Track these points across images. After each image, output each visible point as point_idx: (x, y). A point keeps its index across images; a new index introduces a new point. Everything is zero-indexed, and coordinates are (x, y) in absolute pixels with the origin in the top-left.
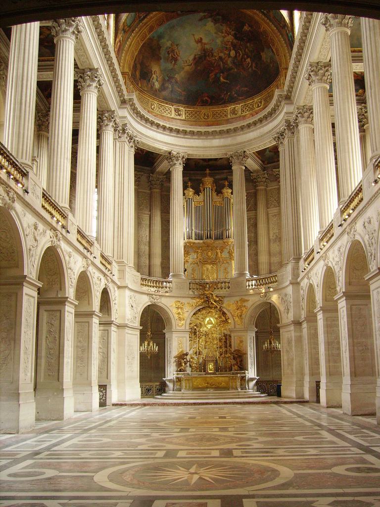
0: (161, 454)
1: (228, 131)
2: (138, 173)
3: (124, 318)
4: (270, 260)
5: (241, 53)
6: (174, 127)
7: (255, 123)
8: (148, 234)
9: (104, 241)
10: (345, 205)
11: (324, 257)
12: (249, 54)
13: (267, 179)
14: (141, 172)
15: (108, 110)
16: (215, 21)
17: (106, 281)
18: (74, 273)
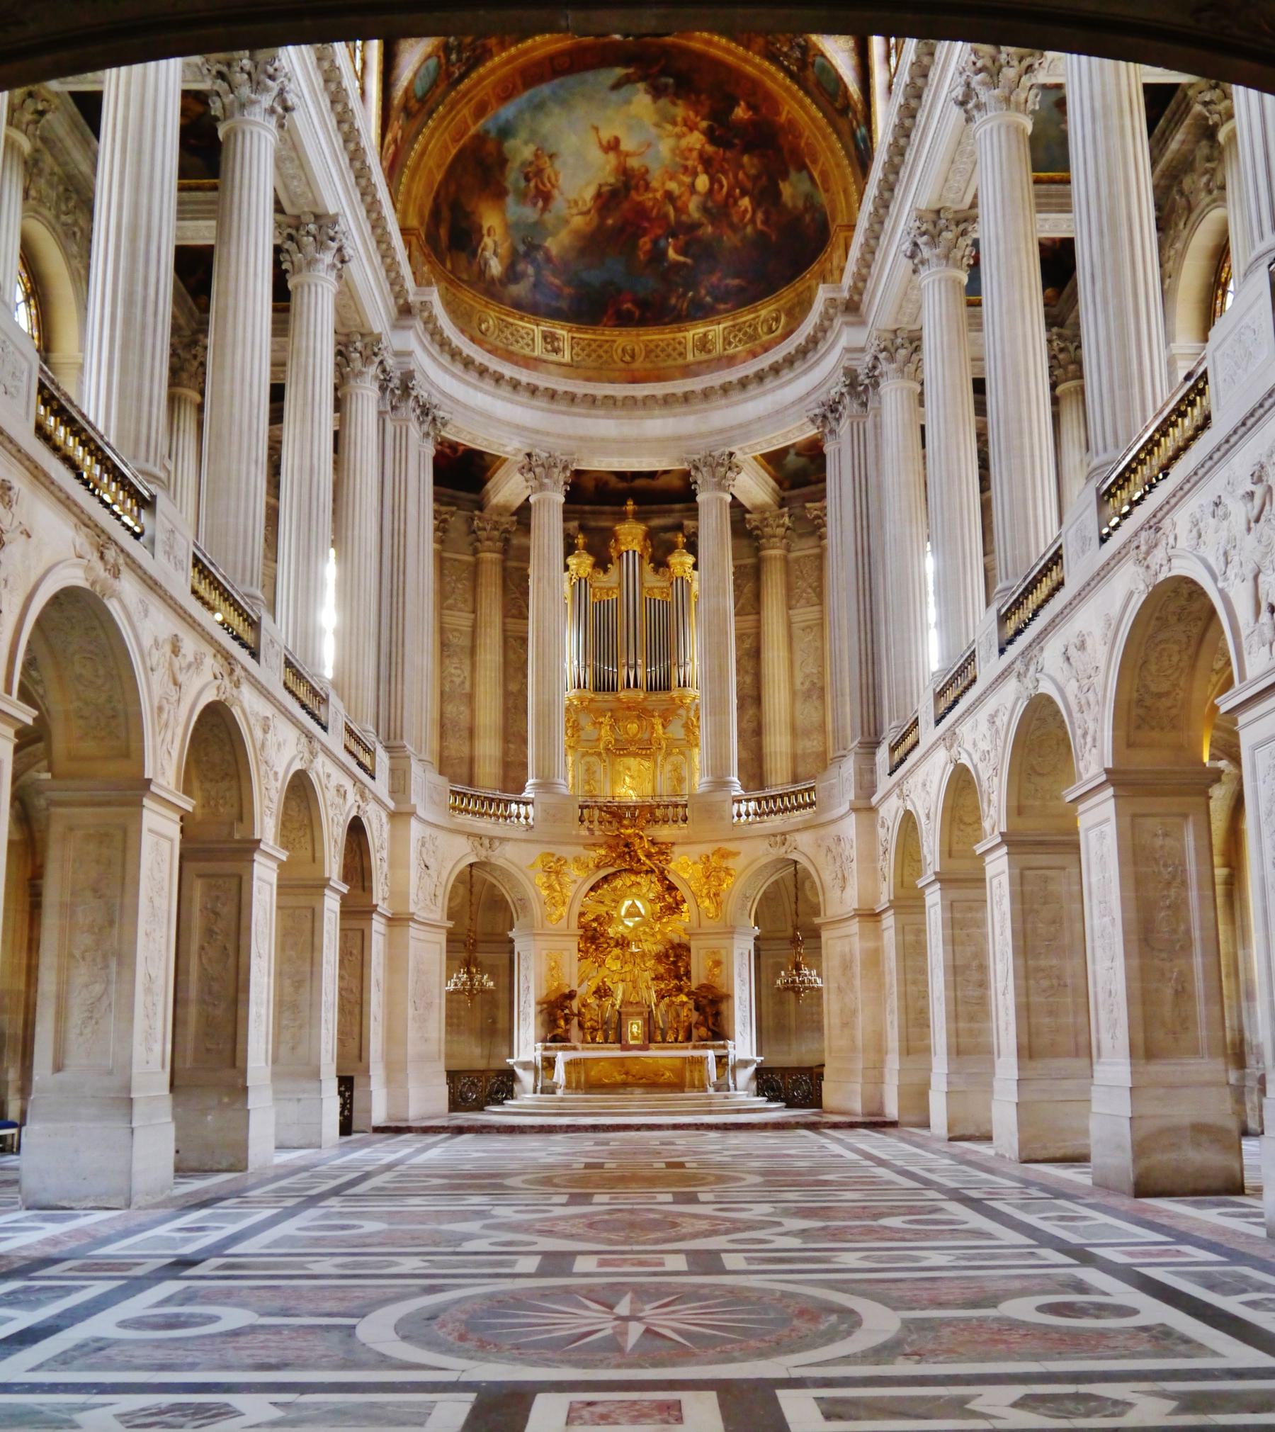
0: (529, 1264)
1: (687, 398)
2: (444, 509)
3: (405, 897)
4: (793, 746)
5: (725, 182)
7: (760, 377)
8: (467, 673)
9: (353, 691)
10: (1011, 601)
11: (950, 739)
12: (749, 185)
13: (788, 528)
14: (449, 504)
15: (363, 331)
16: (657, 92)
17: (358, 798)
18: (276, 773)
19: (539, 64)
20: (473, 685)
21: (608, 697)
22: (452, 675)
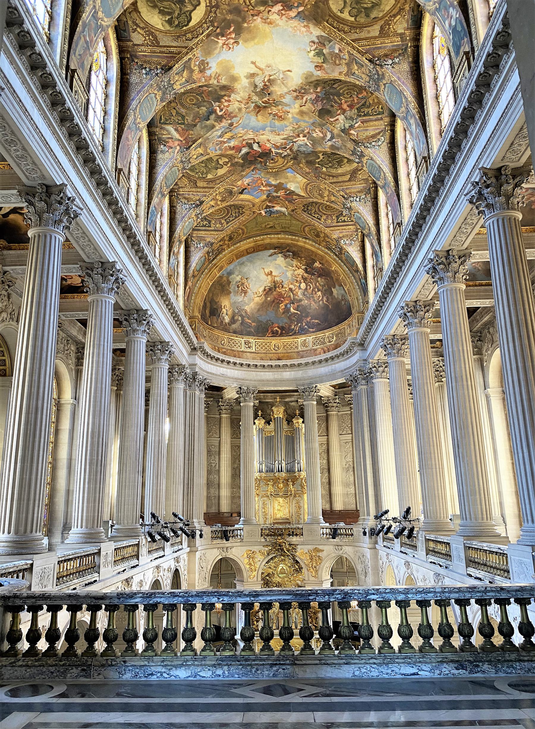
1: (299, 365)
2: (208, 399)
6: (244, 363)
12: (320, 288)
14: (210, 397)
16: (286, 257)
19: (243, 251)
20: (219, 467)
21: (272, 474)
22: (211, 463)
